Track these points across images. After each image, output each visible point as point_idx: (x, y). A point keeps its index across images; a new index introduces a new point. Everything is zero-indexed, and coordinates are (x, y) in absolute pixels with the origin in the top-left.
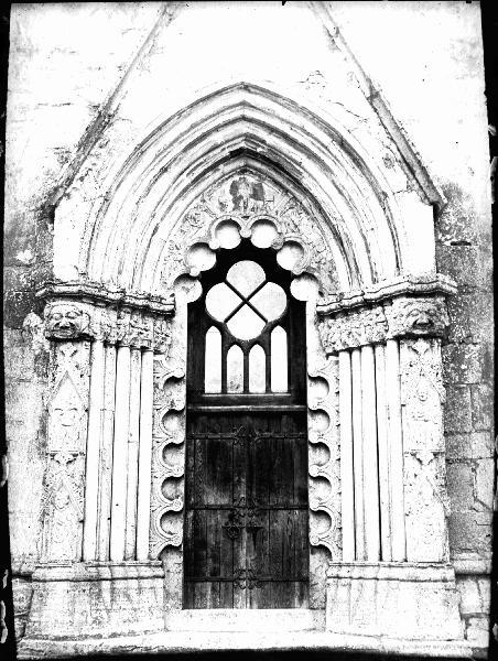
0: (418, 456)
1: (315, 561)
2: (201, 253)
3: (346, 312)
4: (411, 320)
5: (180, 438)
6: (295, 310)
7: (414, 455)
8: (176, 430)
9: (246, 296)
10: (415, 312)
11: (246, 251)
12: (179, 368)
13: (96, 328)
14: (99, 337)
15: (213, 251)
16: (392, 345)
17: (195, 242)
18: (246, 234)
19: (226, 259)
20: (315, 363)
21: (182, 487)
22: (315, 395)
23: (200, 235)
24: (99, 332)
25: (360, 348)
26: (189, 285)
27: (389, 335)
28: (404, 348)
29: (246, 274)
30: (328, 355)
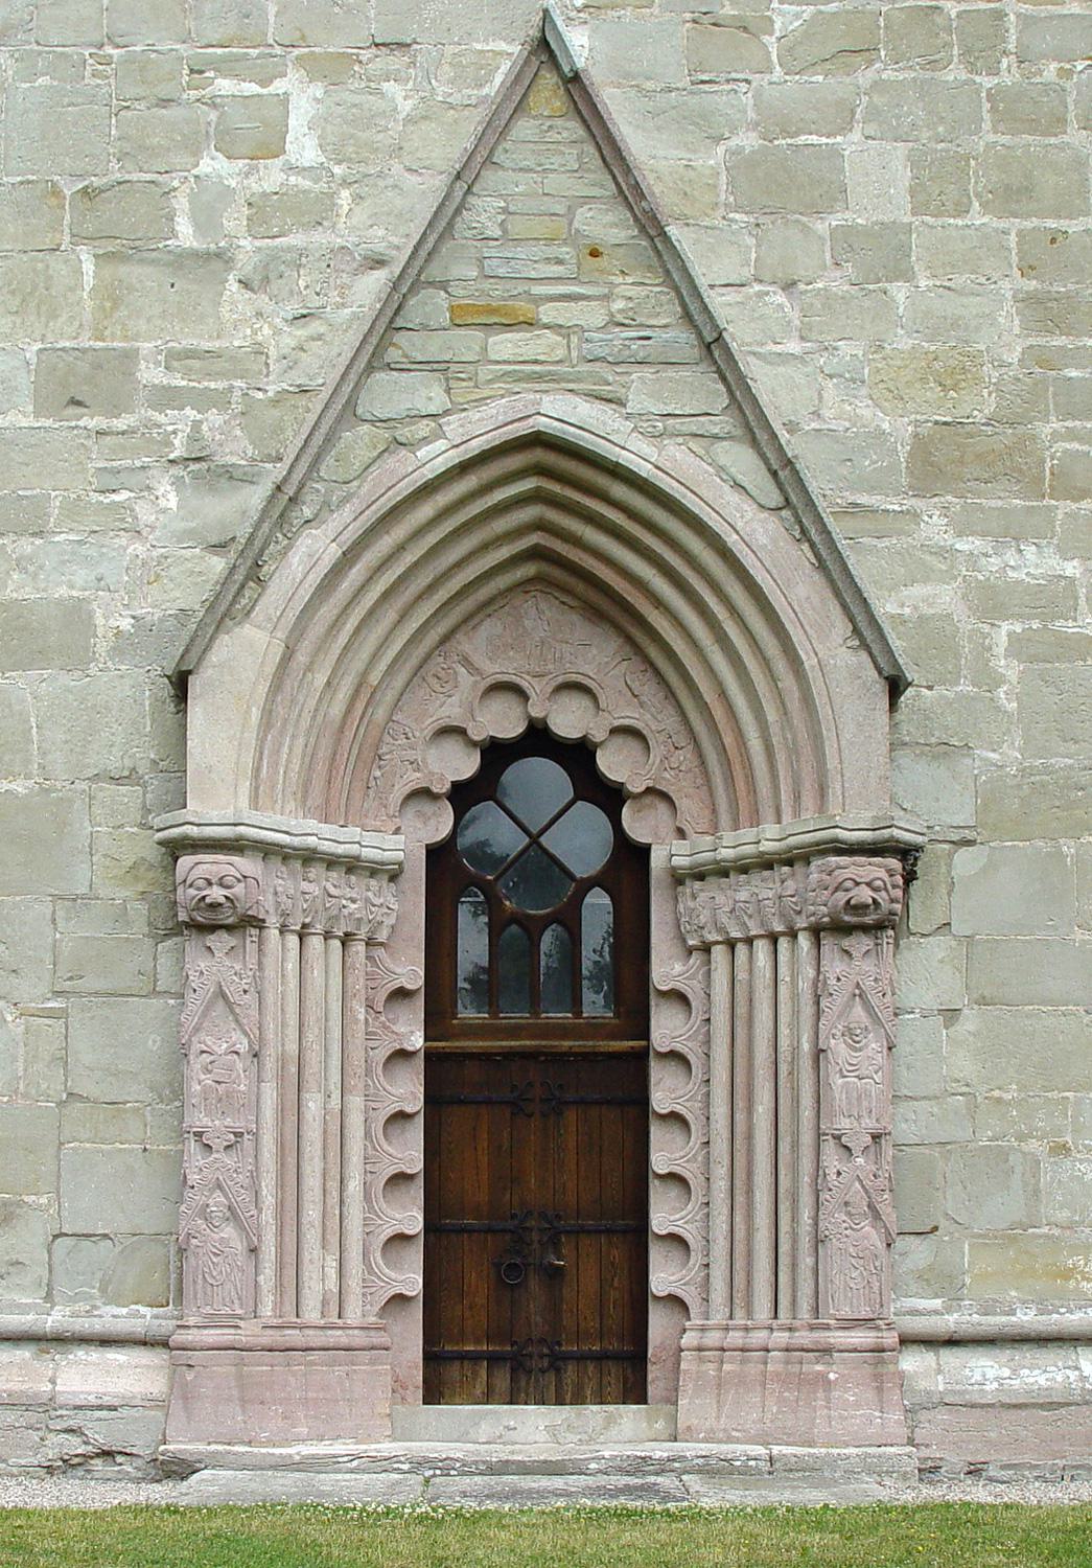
0: (843, 1139)
2: (452, 746)
4: (841, 898)
5: (415, 1104)
6: (630, 859)
7: (837, 1138)
8: (409, 1090)
9: (534, 830)
10: (849, 884)
11: (538, 739)
12: (410, 970)
13: (268, 901)
14: (273, 921)
15: (475, 744)
16: (804, 941)
17: (436, 726)
18: (536, 712)
19: (497, 755)
20: (667, 968)
21: (418, 1191)
22: (666, 1027)
23: (450, 711)
24: (271, 911)
25: (749, 941)
26: (428, 807)
27: (801, 923)
28: (827, 942)
29: (542, 780)
30: (690, 951)
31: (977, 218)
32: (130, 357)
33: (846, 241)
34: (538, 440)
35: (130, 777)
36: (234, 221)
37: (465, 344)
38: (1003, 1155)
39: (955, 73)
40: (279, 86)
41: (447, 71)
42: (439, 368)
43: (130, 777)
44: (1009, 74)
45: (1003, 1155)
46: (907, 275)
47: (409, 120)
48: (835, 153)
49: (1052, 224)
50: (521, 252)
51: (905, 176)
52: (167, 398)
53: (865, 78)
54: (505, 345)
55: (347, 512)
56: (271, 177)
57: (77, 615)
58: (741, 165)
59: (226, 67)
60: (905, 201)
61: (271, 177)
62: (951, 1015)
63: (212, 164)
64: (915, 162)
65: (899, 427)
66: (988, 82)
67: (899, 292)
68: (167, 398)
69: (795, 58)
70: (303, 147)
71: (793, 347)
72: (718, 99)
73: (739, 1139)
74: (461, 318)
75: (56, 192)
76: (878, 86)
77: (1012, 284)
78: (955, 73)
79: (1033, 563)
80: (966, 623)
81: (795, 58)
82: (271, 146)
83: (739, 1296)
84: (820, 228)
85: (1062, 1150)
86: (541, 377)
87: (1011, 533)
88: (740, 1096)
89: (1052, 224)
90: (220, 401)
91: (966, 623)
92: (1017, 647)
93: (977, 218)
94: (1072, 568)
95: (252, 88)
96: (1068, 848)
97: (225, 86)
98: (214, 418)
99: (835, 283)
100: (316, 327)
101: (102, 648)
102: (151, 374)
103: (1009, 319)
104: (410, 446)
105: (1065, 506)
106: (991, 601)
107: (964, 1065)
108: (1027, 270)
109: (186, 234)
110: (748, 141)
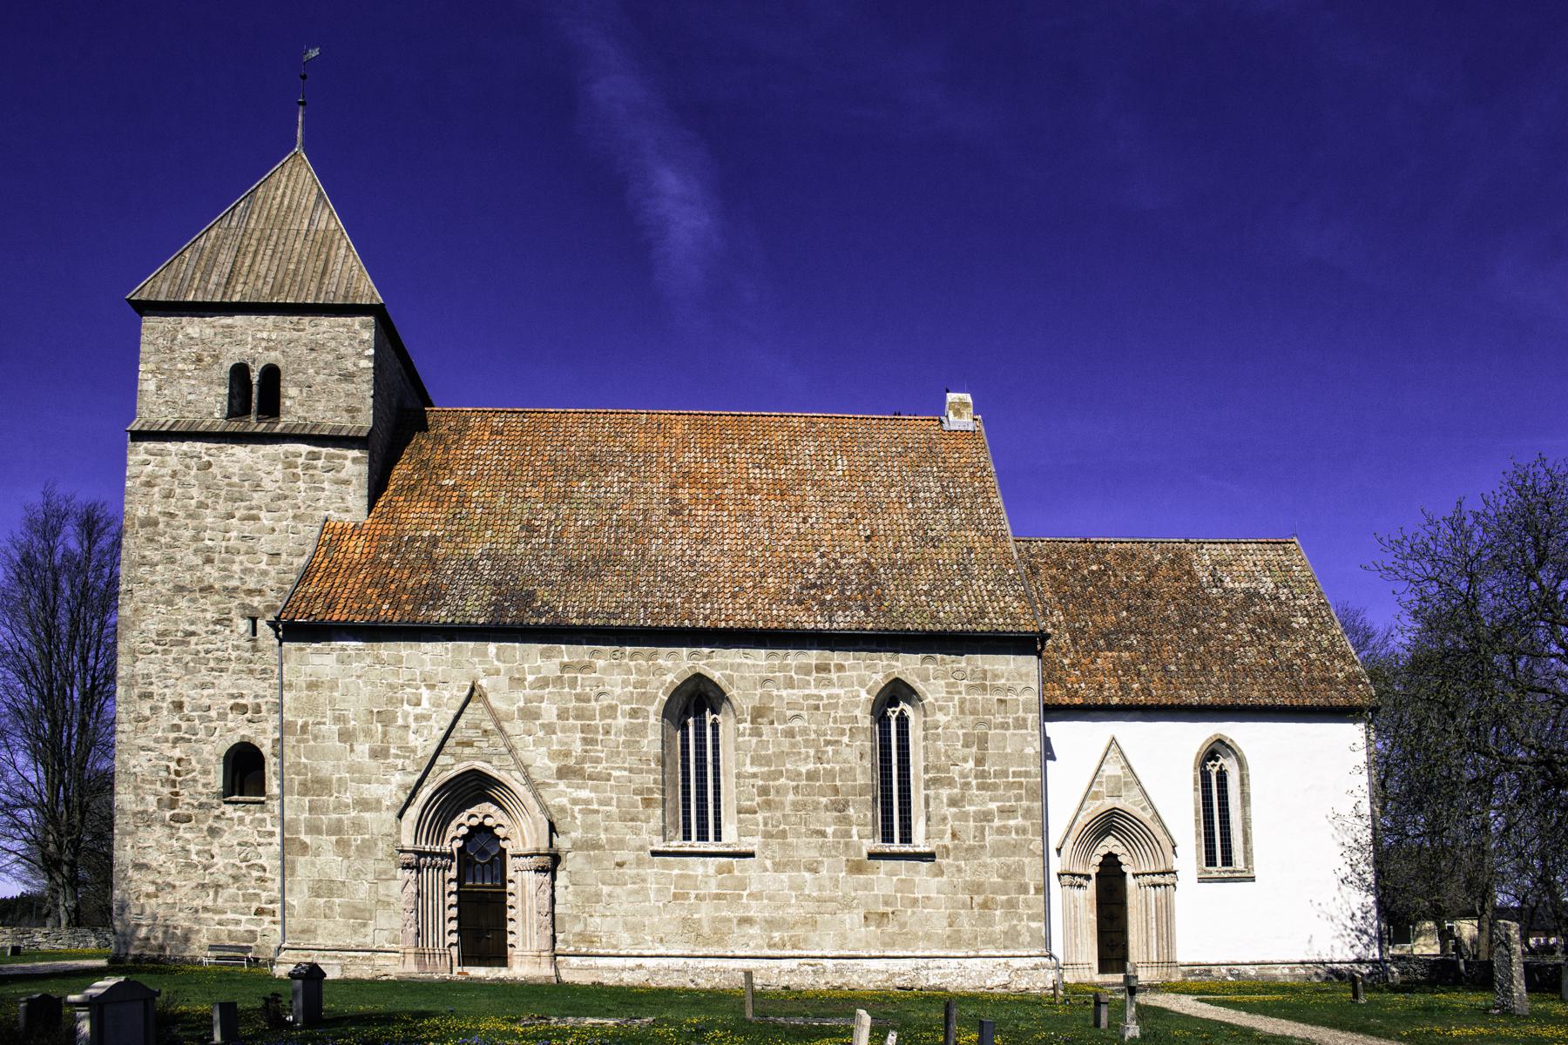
1: (509, 949)
3: (519, 856)
31: (571, 721)
32: (388, 747)
33: (543, 726)
34: (474, 770)
35: (390, 835)
36: (411, 719)
37: (459, 750)
38: (579, 916)
39: (567, 690)
40: (420, 691)
41: (456, 688)
42: (453, 755)
43: (390, 835)
44: (579, 690)
45: (579, 916)
46: (554, 733)
47: (449, 699)
48: (540, 707)
49: (588, 722)
50: (471, 731)
51: (555, 712)
52: (397, 756)
53: (547, 690)
54: (467, 751)
55: (434, 784)
56: (418, 710)
57: (378, 801)
58: (520, 710)
59: (409, 686)
60: (555, 715)
61: (418, 710)
62: (566, 888)
63: (406, 706)
64: (558, 709)
65: (554, 766)
66: (574, 692)
67: (554, 737)
68: (397, 756)
69: (532, 687)
70: (425, 704)
71: (531, 748)
72: (515, 695)
73: (524, 912)
74: (458, 744)
75: (372, 712)
76: (550, 693)
77: (579, 735)
78: (567, 690)
79: (584, 794)
80: (569, 806)
81: (532, 687)
82: (418, 704)
83: (524, 944)
84: (538, 722)
85: (591, 916)
86: (476, 758)
87: (578, 787)
88: (524, 902)
89: (588, 722)
90: (408, 758)
91: (569, 806)
92: (581, 811)
93: (571, 721)
94: (593, 795)
95: (414, 691)
96: (592, 853)
97: (408, 690)
98: (407, 761)
99: (541, 734)
100: (428, 742)
101: (384, 808)
102: (393, 751)
103: (578, 743)
104: (448, 770)
105: (590, 782)
106: (575, 802)
107: (570, 898)
108: (582, 732)
109: (400, 722)
110: (521, 704)
